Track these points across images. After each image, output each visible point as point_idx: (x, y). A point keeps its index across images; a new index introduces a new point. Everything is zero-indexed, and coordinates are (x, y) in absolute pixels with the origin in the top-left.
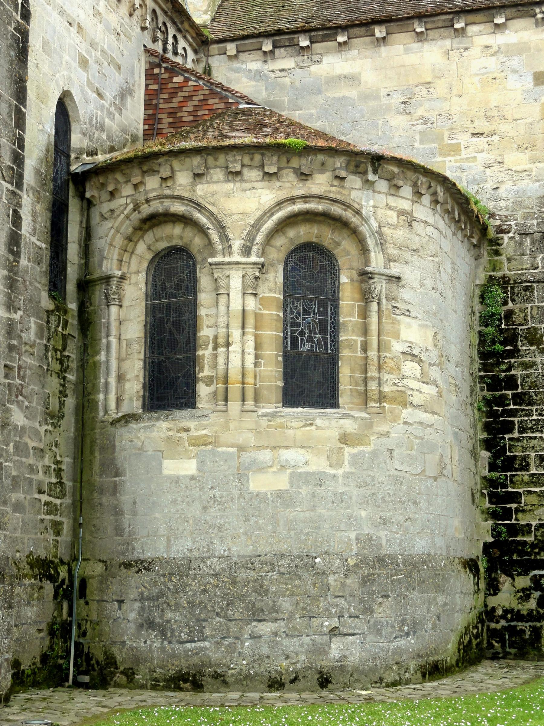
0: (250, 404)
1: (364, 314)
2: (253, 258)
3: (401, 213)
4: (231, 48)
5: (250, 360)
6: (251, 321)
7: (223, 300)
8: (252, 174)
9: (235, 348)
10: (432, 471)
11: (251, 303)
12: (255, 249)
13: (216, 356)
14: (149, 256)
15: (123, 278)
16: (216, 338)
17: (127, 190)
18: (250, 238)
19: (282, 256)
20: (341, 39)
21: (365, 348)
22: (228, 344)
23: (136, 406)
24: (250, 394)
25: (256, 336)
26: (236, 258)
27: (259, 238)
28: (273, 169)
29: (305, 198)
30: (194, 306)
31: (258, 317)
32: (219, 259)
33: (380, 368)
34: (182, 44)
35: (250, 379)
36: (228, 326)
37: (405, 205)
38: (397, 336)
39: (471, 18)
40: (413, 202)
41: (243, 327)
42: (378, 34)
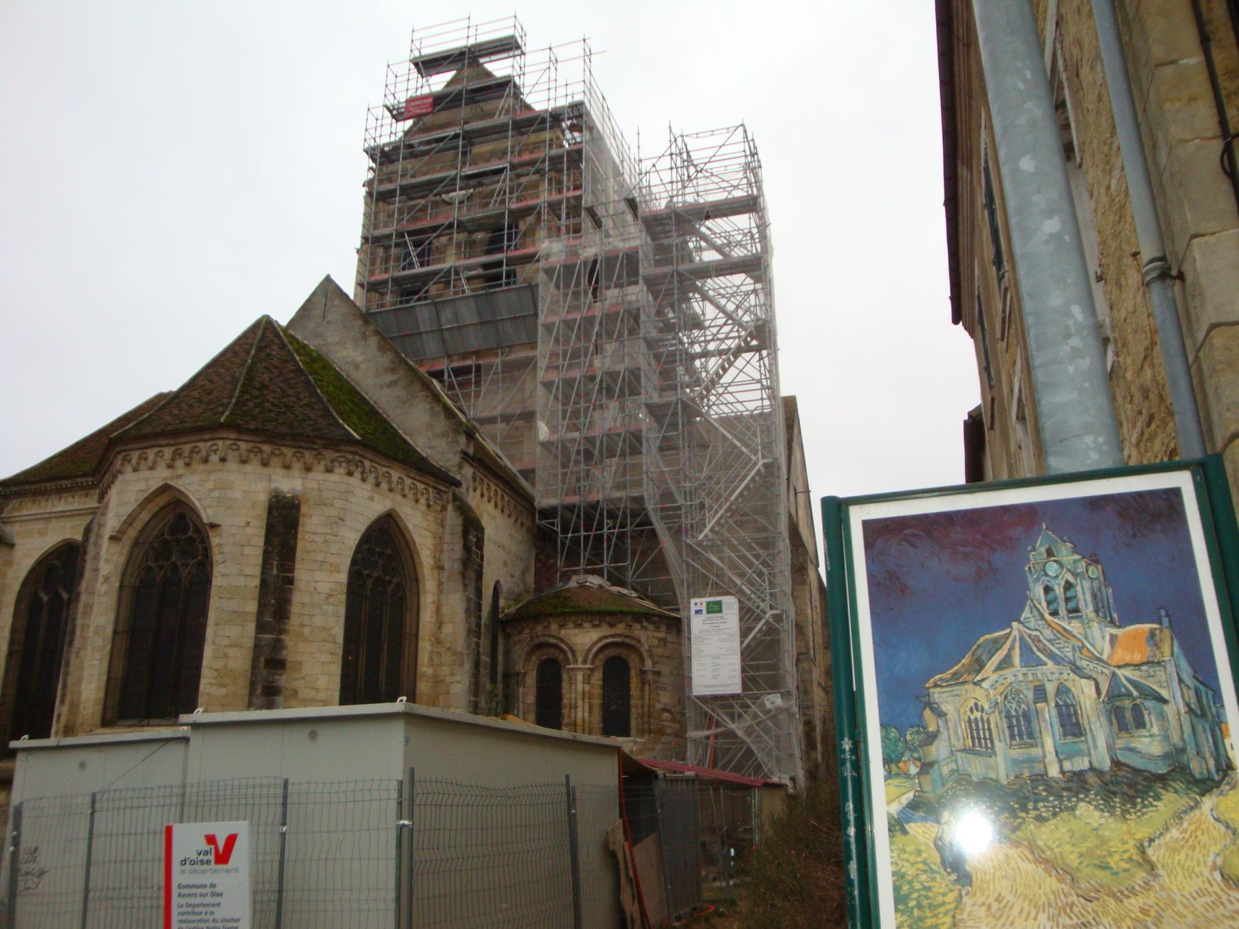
1: (642, 690)
2: (588, 666)
5: (587, 715)
6: (587, 696)
7: (573, 686)
8: (587, 625)
9: (580, 710)
11: (587, 688)
13: (570, 713)
14: (538, 662)
15: (525, 673)
17: (527, 631)
19: (602, 663)
21: (643, 707)
22: (576, 707)
24: (587, 729)
26: (580, 666)
27: (591, 656)
28: (597, 623)
29: (612, 636)
30: (560, 688)
31: (590, 693)
32: (571, 666)
35: (587, 725)
37: (662, 635)
38: (659, 701)
41: (583, 699)
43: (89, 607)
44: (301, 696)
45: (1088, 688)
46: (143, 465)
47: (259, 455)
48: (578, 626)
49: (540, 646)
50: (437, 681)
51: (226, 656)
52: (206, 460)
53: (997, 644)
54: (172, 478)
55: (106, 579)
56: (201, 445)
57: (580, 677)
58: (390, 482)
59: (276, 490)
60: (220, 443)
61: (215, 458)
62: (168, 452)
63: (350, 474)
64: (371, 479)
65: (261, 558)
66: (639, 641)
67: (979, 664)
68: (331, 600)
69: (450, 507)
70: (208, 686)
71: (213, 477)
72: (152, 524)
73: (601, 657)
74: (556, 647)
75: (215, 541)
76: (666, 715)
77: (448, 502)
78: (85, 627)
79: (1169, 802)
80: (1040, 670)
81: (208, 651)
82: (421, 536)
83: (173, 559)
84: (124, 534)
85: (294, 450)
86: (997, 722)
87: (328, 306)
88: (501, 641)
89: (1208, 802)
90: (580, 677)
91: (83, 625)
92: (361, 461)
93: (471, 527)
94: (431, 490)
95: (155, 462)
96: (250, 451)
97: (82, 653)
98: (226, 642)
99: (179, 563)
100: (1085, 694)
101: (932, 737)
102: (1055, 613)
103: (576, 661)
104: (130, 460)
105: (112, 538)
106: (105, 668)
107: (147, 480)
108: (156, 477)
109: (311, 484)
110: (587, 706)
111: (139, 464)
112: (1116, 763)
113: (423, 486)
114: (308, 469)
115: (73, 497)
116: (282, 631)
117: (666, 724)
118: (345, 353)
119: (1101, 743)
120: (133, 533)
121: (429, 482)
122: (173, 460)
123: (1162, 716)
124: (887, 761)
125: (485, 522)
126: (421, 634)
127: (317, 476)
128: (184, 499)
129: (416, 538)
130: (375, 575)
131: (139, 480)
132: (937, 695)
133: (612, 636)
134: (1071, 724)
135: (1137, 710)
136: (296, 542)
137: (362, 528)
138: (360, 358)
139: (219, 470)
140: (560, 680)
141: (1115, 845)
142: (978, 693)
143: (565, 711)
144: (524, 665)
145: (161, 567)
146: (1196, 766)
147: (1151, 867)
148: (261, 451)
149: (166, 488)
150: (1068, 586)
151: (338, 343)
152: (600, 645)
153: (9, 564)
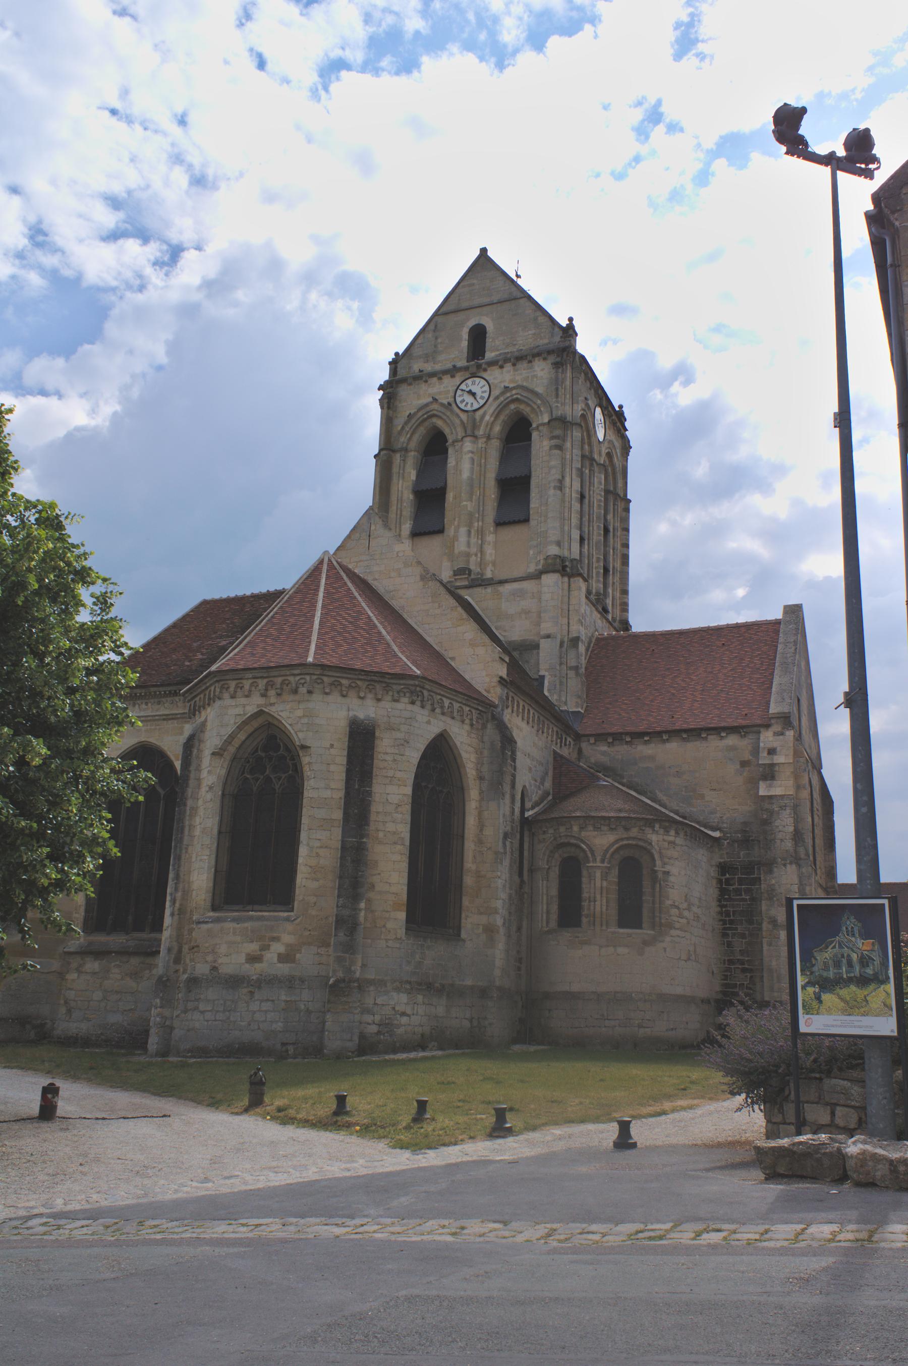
0: (604, 928)
2: (606, 864)
3: (670, 842)
4: (592, 740)
5: (604, 908)
7: (592, 882)
8: (605, 828)
12: (606, 860)
13: (590, 905)
16: (590, 897)
20: (646, 738)
21: (654, 903)
22: (595, 901)
23: (553, 924)
25: (607, 898)
26: (599, 864)
27: (608, 856)
29: (628, 839)
30: (580, 882)
32: (591, 864)
33: (660, 912)
34: (569, 739)
36: (595, 893)
37: (671, 838)
39: (709, 732)
40: (675, 837)
41: (601, 894)
42: (664, 738)
43: (194, 810)
44: (377, 888)
46: (239, 693)
47: (339, 688)
48: (596, 829)
51: (318, 855)
52: (295, 692)
53: (832, 942)
54: (266, 705)
55: (211, 788)
56: (291, 679)
57: (598, 874)
58: (442, 707)
60: (308, 678)
61: (303, 690)
62: (262, 683)
63: (413, 703)
64: (429, 707)
65: (344, 775)
66: (650, 844)
67: (827, 947)
68: (400, 809)
70: (304, 880)
71: (302, 706)
75: (305, 760)
76: (674, 911)
77: (487, 721)
78: (191, 827)
79: (872, 986)
80: (843, 950)
81: (303, 851)
83: (267, 772)
84: (224, 751)
85: (367, 683)
86: (831, 962)
88: (526, 839)
89: (882, 986)
90: (598, 874)
91: (190, 826)
92: (421, 691)
93: (508, 741)
94: (474, 711)
95: (250, 691)
96: (332, 684)
97: (190, 848)
98: (318, 844)
99: (272, 777)
100: (854, 957)
101: (813, 965)
102: (848, 935)
103: (595, 860)
104: (228, 688)
105: (213, 754)
106: (213, 862)
107: (244, 706)
108: (253, 704)
110: (605, 901)
111: (235, 692)
112: (861, 975)
113: (468, 709)
114: (379, 700)
115: (147, 704)
116: (362, 836)
117: (675, 919)
119: (858, 970)
120: (232, 749)
121: (472, 705)
122: (266, 690)
123: (873, 964)
124: (802, 970)
125: (516, 734)
126: (466, 836)
127: (387, 704)
128: (276, 723)
129: (464, 755)
130: (430, 786)
131: (236, 706)
132: (816, 954)
133: (628, 839)
136: (373, 761)
137: (422, 747)
140: (579, 875)
141: (859, 996)
142: (826, 955)
143: (585, 904)
144: (548, 861)
145: (257, 779)
146: (880, 977)
147: (867, 1001)
148: (341, 684)
149: (260, 713)
150: (852, 928)
152: (617, 846)
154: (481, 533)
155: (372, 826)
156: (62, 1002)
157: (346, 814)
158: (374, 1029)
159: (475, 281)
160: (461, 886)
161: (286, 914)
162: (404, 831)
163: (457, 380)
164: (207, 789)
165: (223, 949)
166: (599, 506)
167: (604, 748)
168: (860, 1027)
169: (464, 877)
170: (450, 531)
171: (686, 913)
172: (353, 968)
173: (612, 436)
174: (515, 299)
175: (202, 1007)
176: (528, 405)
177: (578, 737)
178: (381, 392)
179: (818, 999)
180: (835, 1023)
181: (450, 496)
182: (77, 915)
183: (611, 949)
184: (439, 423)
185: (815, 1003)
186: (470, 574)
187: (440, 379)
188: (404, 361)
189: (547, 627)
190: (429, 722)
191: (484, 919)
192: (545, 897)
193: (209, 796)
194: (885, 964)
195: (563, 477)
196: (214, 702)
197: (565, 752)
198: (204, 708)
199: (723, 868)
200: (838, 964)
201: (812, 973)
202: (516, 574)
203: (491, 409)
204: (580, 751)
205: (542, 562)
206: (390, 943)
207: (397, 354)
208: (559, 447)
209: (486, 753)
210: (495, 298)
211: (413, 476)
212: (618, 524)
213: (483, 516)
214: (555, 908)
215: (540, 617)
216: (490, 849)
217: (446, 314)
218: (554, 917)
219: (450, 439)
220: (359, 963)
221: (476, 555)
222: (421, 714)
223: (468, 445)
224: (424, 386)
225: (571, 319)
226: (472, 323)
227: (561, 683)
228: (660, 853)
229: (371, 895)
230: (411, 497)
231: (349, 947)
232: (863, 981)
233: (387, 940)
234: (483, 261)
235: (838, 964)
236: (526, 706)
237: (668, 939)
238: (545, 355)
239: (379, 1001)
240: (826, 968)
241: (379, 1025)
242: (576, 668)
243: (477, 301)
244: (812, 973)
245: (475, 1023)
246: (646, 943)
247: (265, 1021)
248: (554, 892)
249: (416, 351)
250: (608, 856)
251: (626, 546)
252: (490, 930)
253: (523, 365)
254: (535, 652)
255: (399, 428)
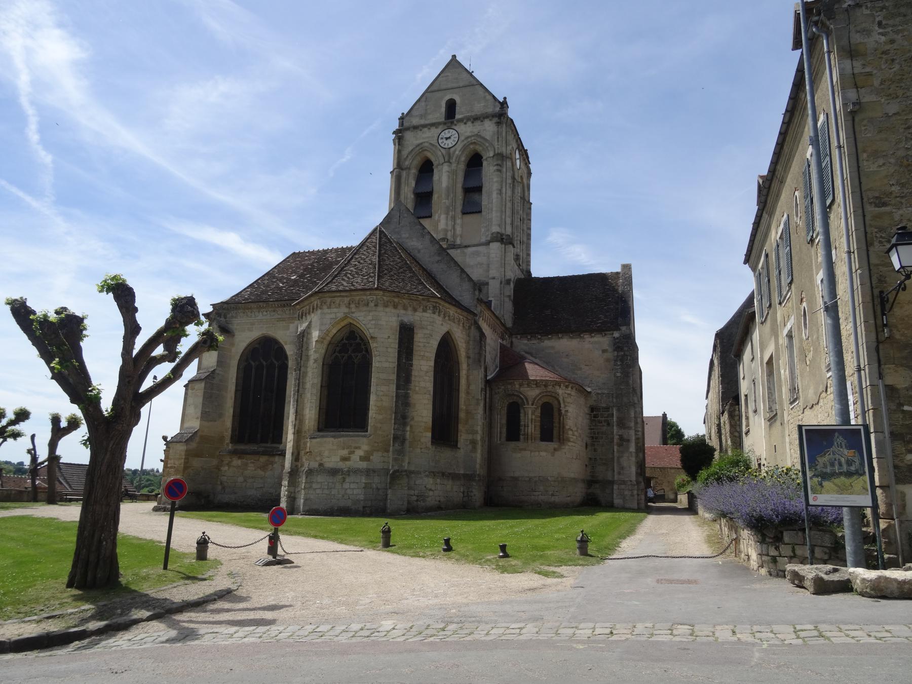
0: (533, 441)
3: (568, 394)
4: (519, 337)
6: (533, 421)
9: (530, 428)
10: (575, 457)
13: (525, 429)
16: (525, 425)
18: (534, 401)
21: (559, 428)
23: (504, 439)
37: (569, 392)
45: (843, 459)
46: (333, 305)
49: (510, 395)
50: (468, 412)
51: (382, 400)
57: (530, 412)
58: (449, 316)
59: (402, 320)
61: (372, 304)
62: (346, 300)
63: (434, 313)
64: (442, 316)
65: (397, 354)
66: (558, 395)
67: (825, 454)
69: (473, 327)
72: (338, 335)
73: (540, 402)
74: (518, 396)
75: (373, 345)
77: (471, 325)
81: (373, 398)
82: (460, 342)
87: (401, 217)
88: (488, 392)
90: (530, 412)
91: (303, 382)
93: (482, 335)
98: (381, 393)
100: (843, 460)
103: (528, 404)
106: (318, 404)
107: (336, 313)
109: (417, 318)
110: (533, 426)
111: (330, 305)
116: (408, 389)
117: (571, 436)
118: (412, 244)
120: (328, 339)
122: (349, 304)
132: (818, 458)
134: (840, 464)
135: (851, 463)
137: (439, 339)
138: (420, 247)
139: (375, 311)
140: (519, 412)
143: (522, 428)
146: (860, 472)
147: (852, 486)
149: (346, 317)
151: (408, 238)
153: (233, 345)
154: (454, 218)
155: (413, 384)
156: (219, 483)
157: (398, 376)
158: (415, 498)
159: (449, 74)
160: (458, 417)
161: (363, 434)
162: (430, 386)
163: (439, 130)
164: (313, 361)
165: (326, 453)
166: (518, 206)
167: (526, 342)
168: (848, 501)
169: (460, 413)
170: (436, 217)
171: (576, 433)
172: (403, 464)
173: (523, 166)
174: (473, 85)
175: (315, 486)
176: (481, 146)
177: (511, 335)
178: (394, 135)
179: (821, 485)
180: (832, 499)
181: (435, 197)
182: (226, 434)
183: (537, 453)
184: (429, 155)
185: (819, 487)
186: (447, 242)
187: (429, 129)
188: (407, 118)
189: (493, 272)
190: (442, 325)
191: (470, 437)
192: (499, 424)
193: (315, 365)
194: (862, 464)
195: (502, 188)
196: (317, 310)
197: (504, 343)
198: (309, 313)
199: (592, 409)
200: (832, 465)
201: (816, 470)
202: (476, 242)
203: (459, 146)
204: (512, 342)
205: (490, 236)
206: (423, 450)
207: (403, 114)
208: (499, 171)
209: (471, 342)
210: (461, 84)
211: (413, 183)
212: (525, 216)
213: (455, 208)
214: (504, 430)
215: (489, 267)
216: (473, 397)
217: (433, 92)
218: (504, 435)
219: (435, 163)
220: (407, 461)
221: (451, 231)
222: (438, 319)
223: (446, 168)
224: (419, 132)
225: (505, 98)
226: (448, 97)
227: (501, 304)
228: (563, 400)
229: (412, 423)
230: (412, 196)
231: (400, 452)
232: (849, 474)
233: (421, 448)
234: (454, 63)
235: (832, 465)
236: (489, 317)
237: (567, 447)
238: (490, 118)
239: (417, 483)
240: (825, 466)
241: (418, 496)
242: (509, 296)
243: (450, 86)
244: (816, 470)
245: (466, 494)
246: (555, 450)
247: (353, 494)
248: (504, 421)
249: (414, 113)
250: (535, 401)
251: (530, 229)
252: (473, 443)
253: (478, 123)
254: (486, 286)
255: (405, 157)
